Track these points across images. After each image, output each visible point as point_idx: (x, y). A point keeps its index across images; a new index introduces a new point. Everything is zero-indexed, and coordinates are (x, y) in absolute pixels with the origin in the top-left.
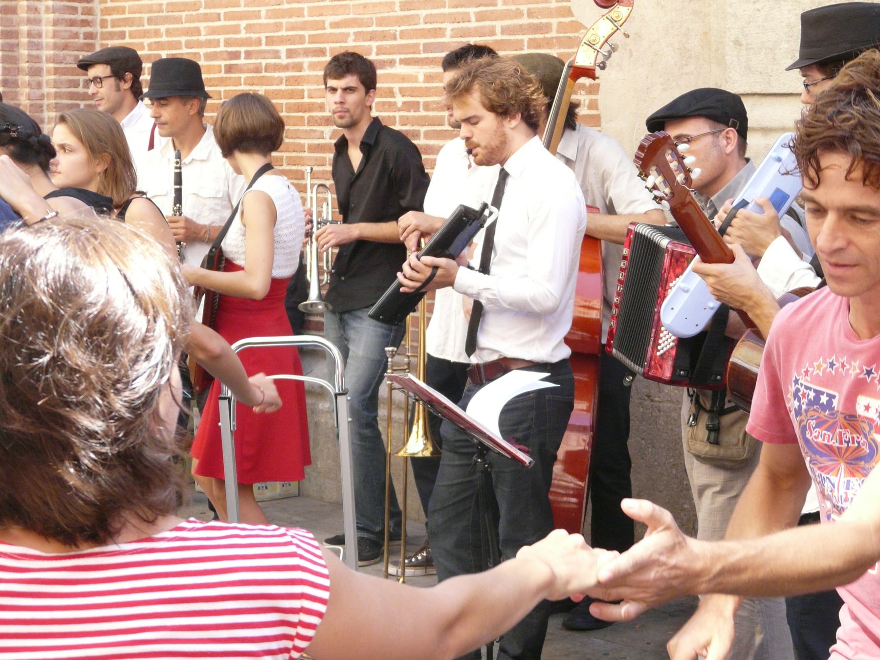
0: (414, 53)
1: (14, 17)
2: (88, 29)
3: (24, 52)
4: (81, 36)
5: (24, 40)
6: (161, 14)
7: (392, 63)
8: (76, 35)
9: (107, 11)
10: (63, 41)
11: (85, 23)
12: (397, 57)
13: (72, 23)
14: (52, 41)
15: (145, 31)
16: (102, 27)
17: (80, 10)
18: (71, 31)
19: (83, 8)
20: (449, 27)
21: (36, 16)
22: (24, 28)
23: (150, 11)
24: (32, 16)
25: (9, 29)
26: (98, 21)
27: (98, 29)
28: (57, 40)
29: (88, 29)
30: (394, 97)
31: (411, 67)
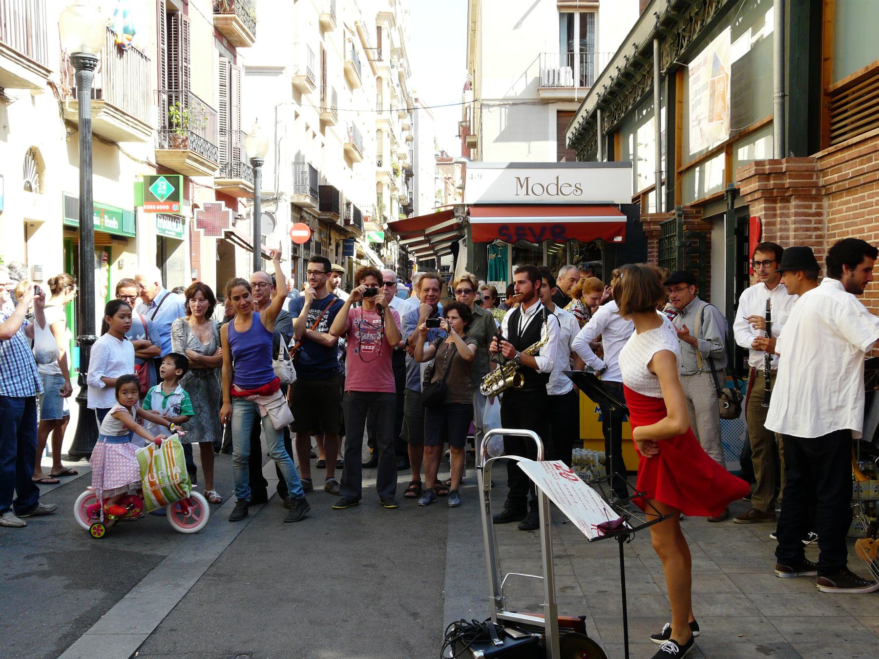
2: (819, 233)
8: (810, 237)
9: (830, 221)
13: (808, 230)
15: (844, 232)
22: (779, 234)
29: (819, 233)
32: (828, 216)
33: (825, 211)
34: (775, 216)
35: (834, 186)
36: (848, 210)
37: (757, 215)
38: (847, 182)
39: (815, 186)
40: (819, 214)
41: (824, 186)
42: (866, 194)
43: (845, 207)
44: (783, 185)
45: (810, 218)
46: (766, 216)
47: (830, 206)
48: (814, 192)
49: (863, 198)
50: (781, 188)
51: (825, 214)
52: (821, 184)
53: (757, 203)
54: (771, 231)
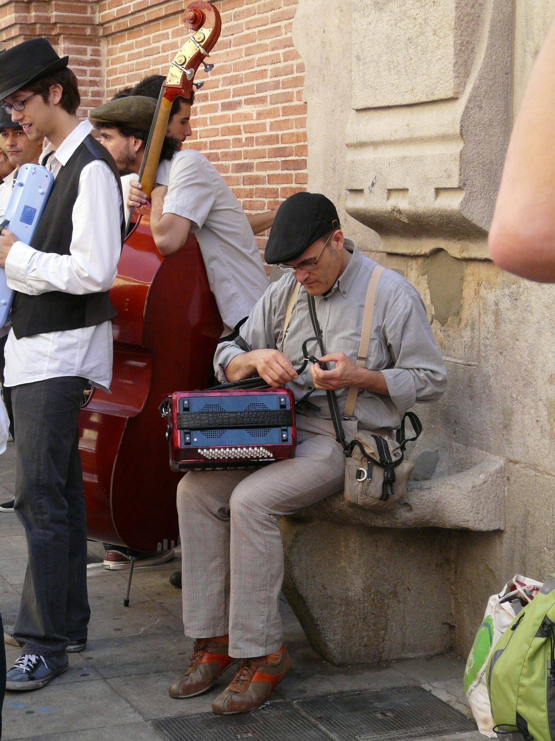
0: (251, 94)
2: (96, 88)
4: (90, 94)
6: (133, 73)
7: (239, 103)
9: (110, 73)
12: (242, 98)
16: (108, 86)
17: (88, 73)
19: (92, 71)
20: (269, 67)
23: (128, 71)
26: (105, 81)
27: (105, 88)
29: (96, 88)
30: (241, 134)
31: (250, 106)
32: (108, 65)
33: (103, 59)
35: (113, 24)
36: (132, 57)
38: (128, 19)
39: (90, 23)
40: (96, 63)
41: (101, 25)
42: (151, 36)
43: (126, 54)
44: (48, 19)
45: (85, 68)
47: (110, 53)
48: (88, 32)
49: (147, 42)
50: (46, 22)
51: (104, 64)
52: (97, 22)
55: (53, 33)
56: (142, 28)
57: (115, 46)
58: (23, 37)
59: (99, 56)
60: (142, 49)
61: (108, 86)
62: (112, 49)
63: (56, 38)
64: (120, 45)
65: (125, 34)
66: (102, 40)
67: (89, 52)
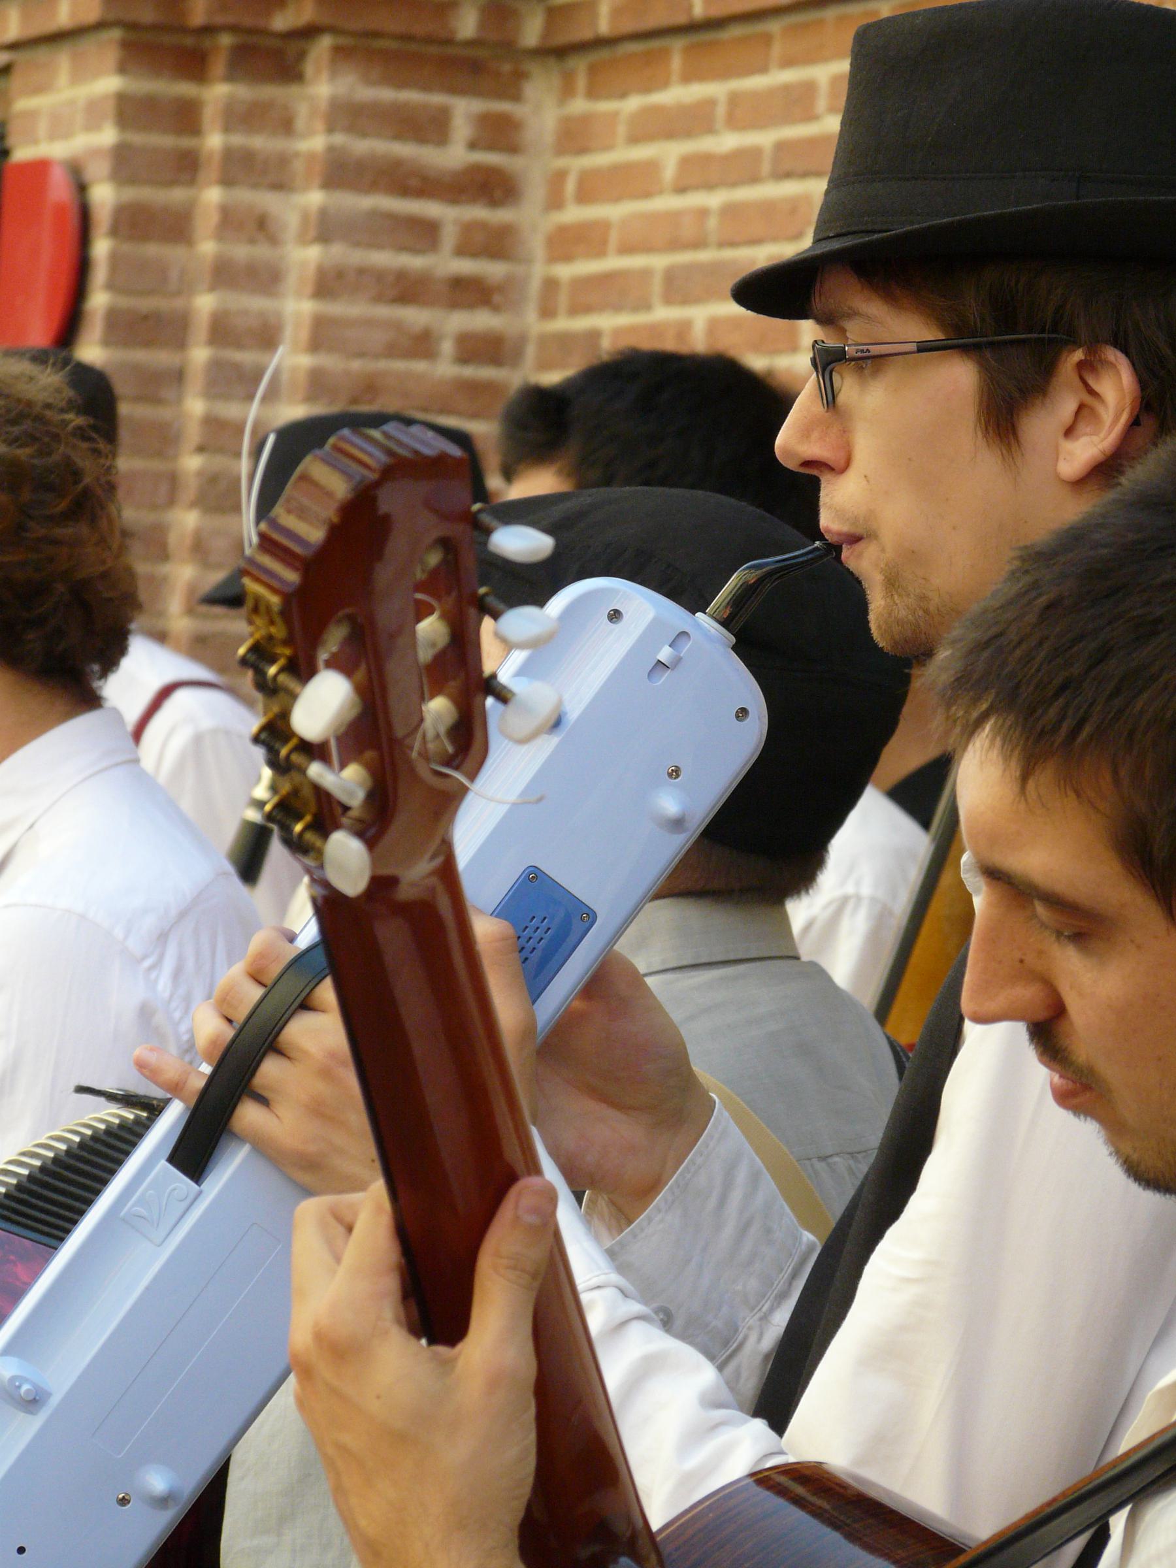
1: (173, 254)
2: (481, 320)
3: (195, 406)
4: (447, 347)
5: (200, 355)
6: (704, 256)
8: (422, 344)
9: (568, 242)
10: (356, 365)
11: (469, 292)
13: (408, 290)
14: (305, 361)
17: (449, 237)
18: (397, 326)
19: (468, 228)
21: (261, 252)
22: (205, 303)
23: (675, 245)
24: (241, 252)
25: (145, 304)
26: (534, 287)
27: (531, 323)
28: (330, 361)
29: (481, 320)
32: (555, 202)
33: (533, 168)
34: (187, 166)
36: (700, 173)
37: (57, 150)
40: (493, 187)
43: (669, 154)
45: (431, 209)
46: (123, 162)
47: (575, 137)
51: (535, 192)
53: (62, 60)
54: (156, 278)
55: (281, 22)
56: (774, 26)
57: (605, 106)
58: (116, 34)
59: (513, 149)
60: (764, 139)
61: (547, 311)
62: (585, 120)
63: (292, 47)
64: (633, 103)
65: (665, 53)
66: (534, 68)
67: (462, 128)
